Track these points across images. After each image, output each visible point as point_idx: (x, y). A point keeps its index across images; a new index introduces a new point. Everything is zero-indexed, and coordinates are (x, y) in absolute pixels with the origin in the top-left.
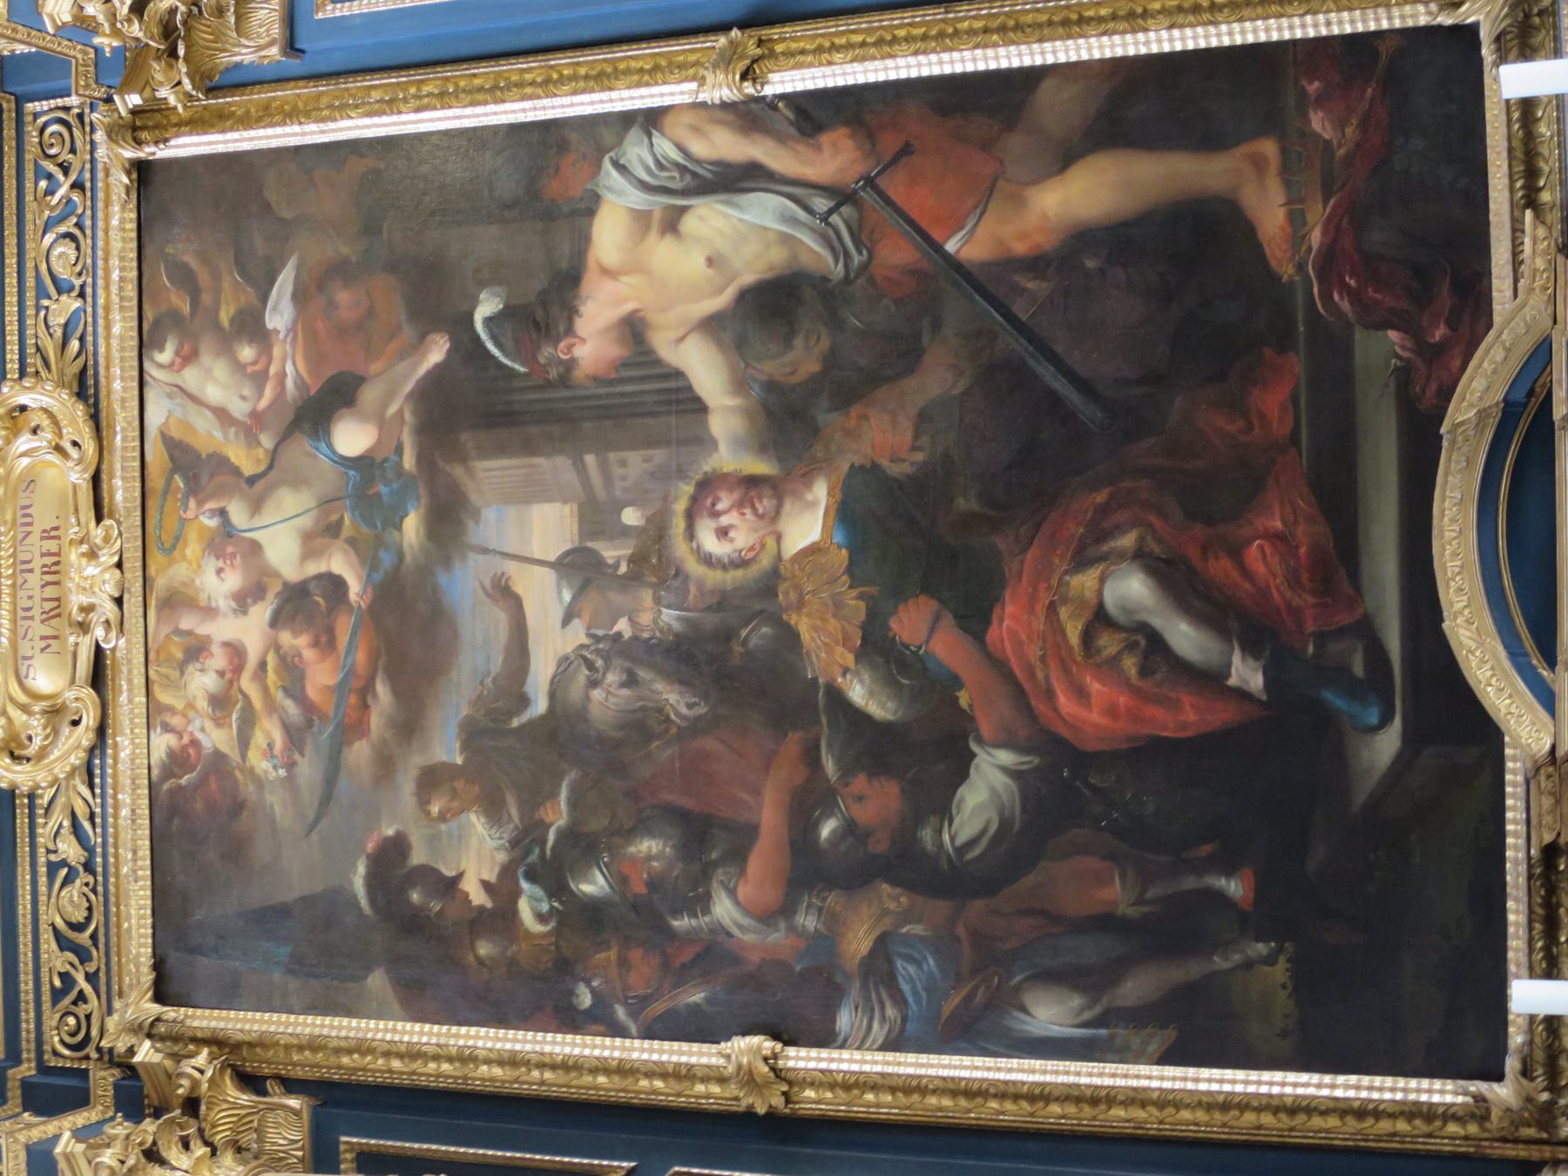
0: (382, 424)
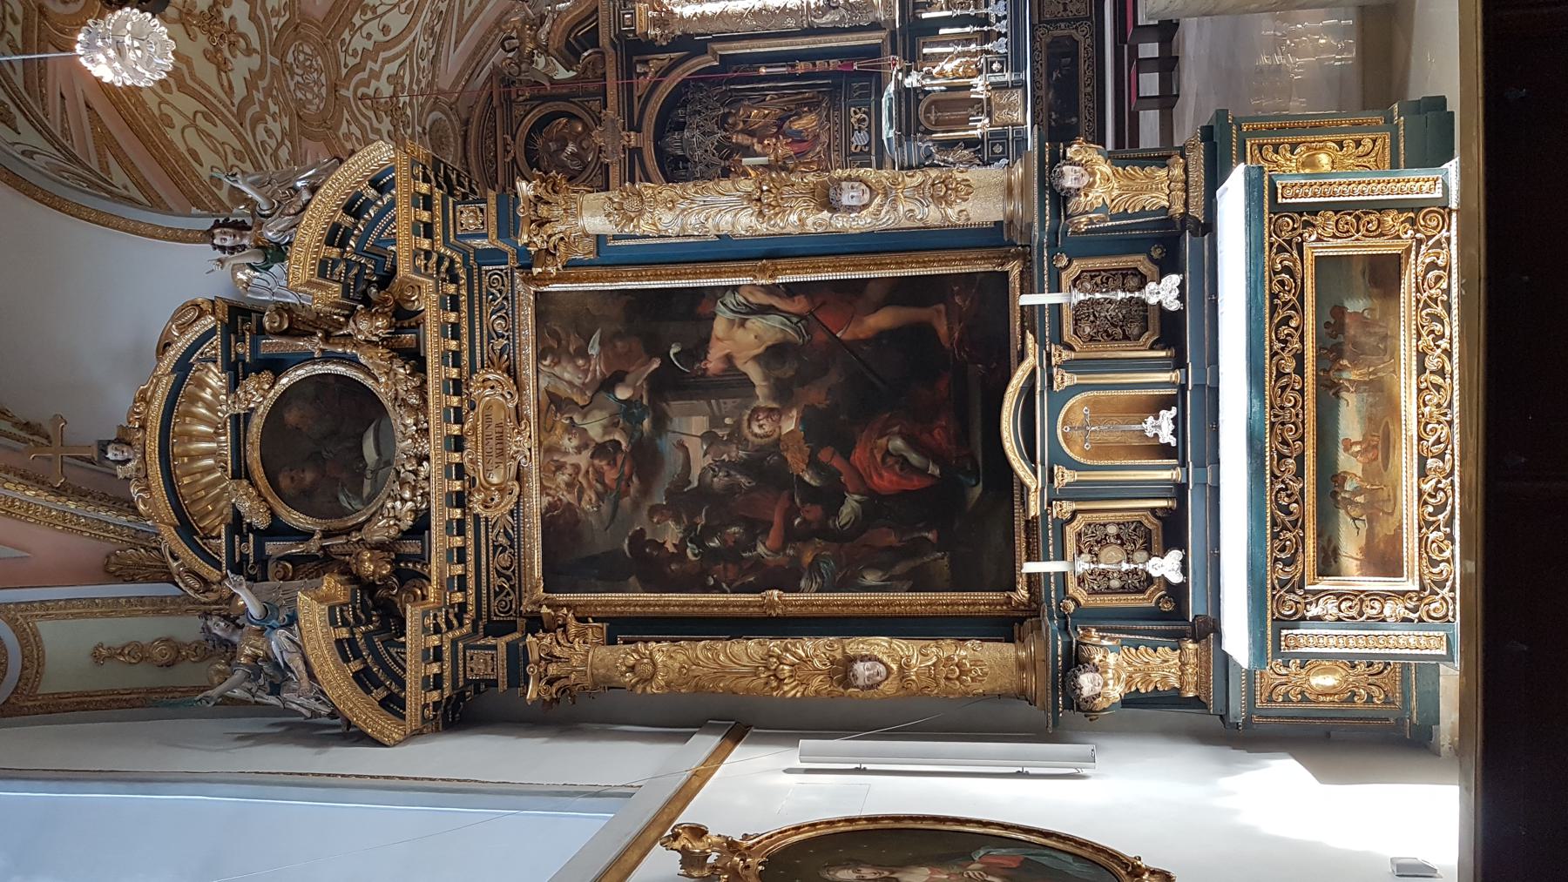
0: (634, 388)
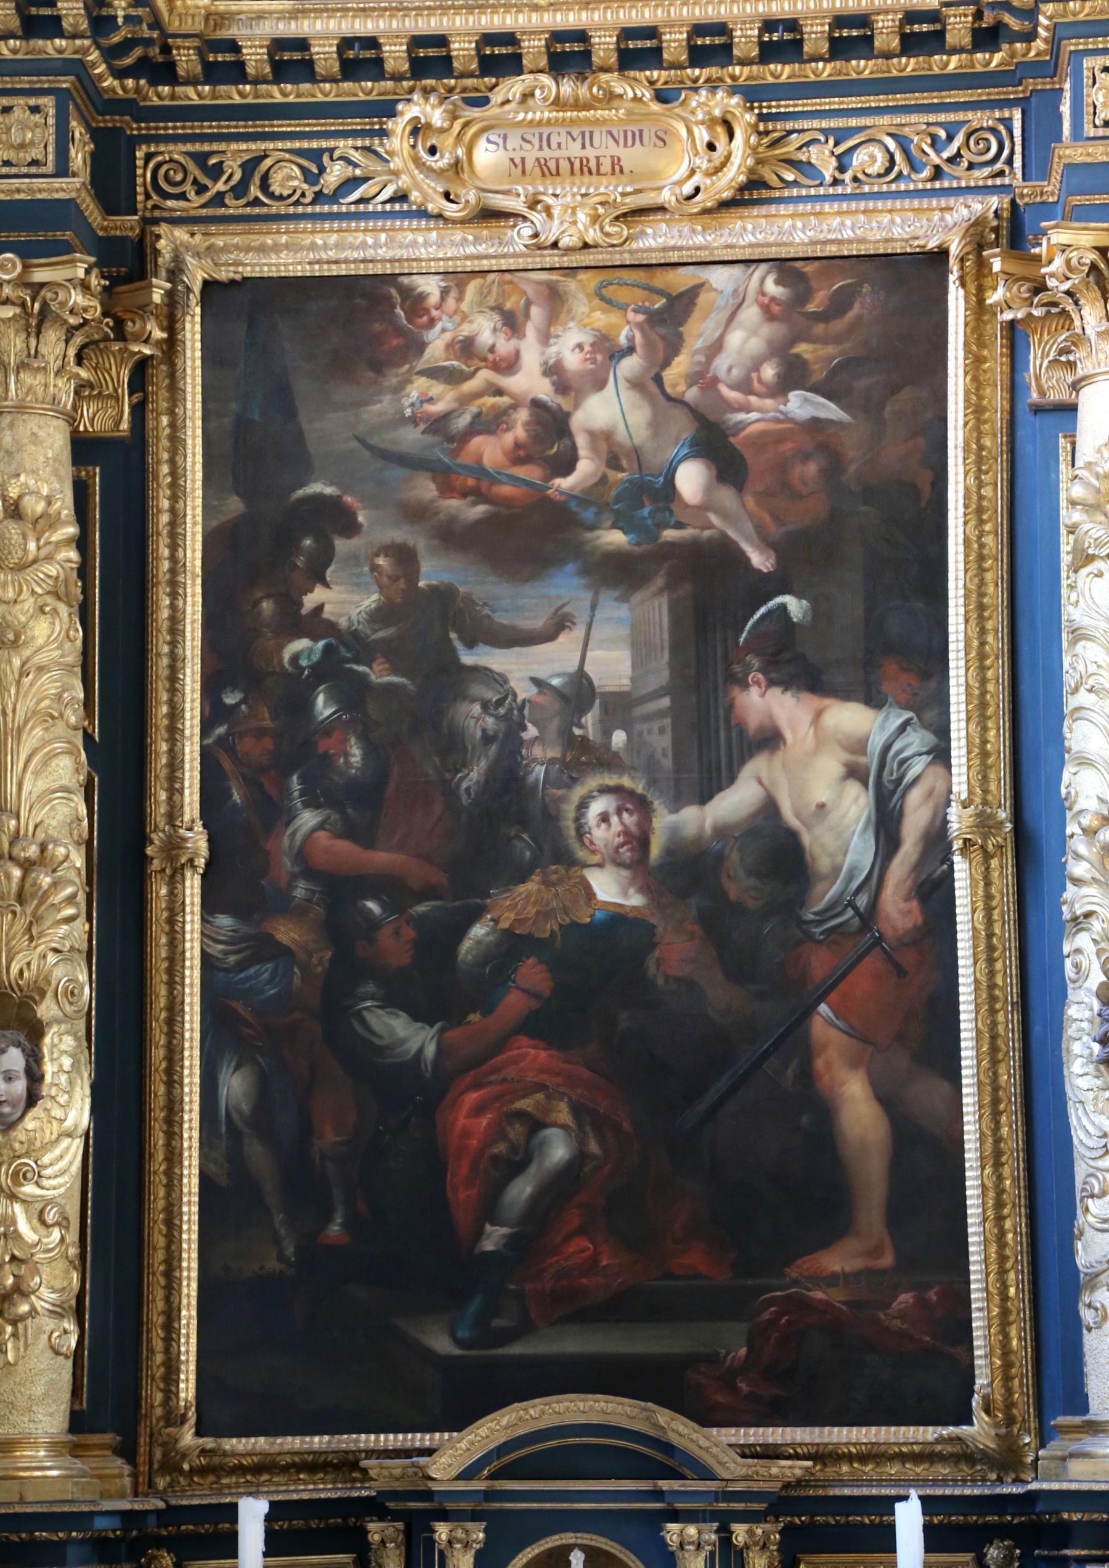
0: (704, 507)
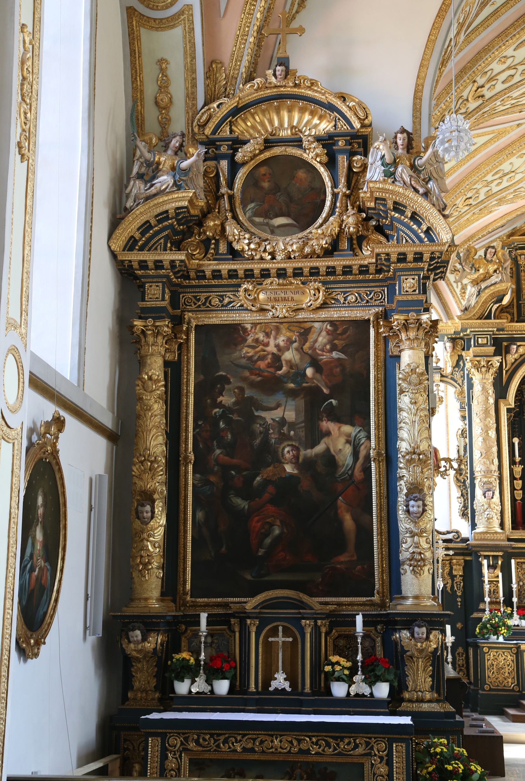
0: (312, 379)
